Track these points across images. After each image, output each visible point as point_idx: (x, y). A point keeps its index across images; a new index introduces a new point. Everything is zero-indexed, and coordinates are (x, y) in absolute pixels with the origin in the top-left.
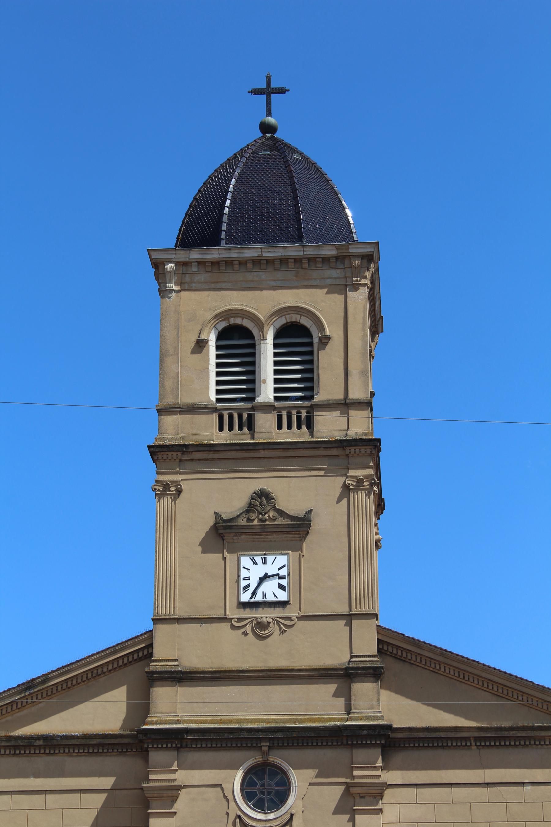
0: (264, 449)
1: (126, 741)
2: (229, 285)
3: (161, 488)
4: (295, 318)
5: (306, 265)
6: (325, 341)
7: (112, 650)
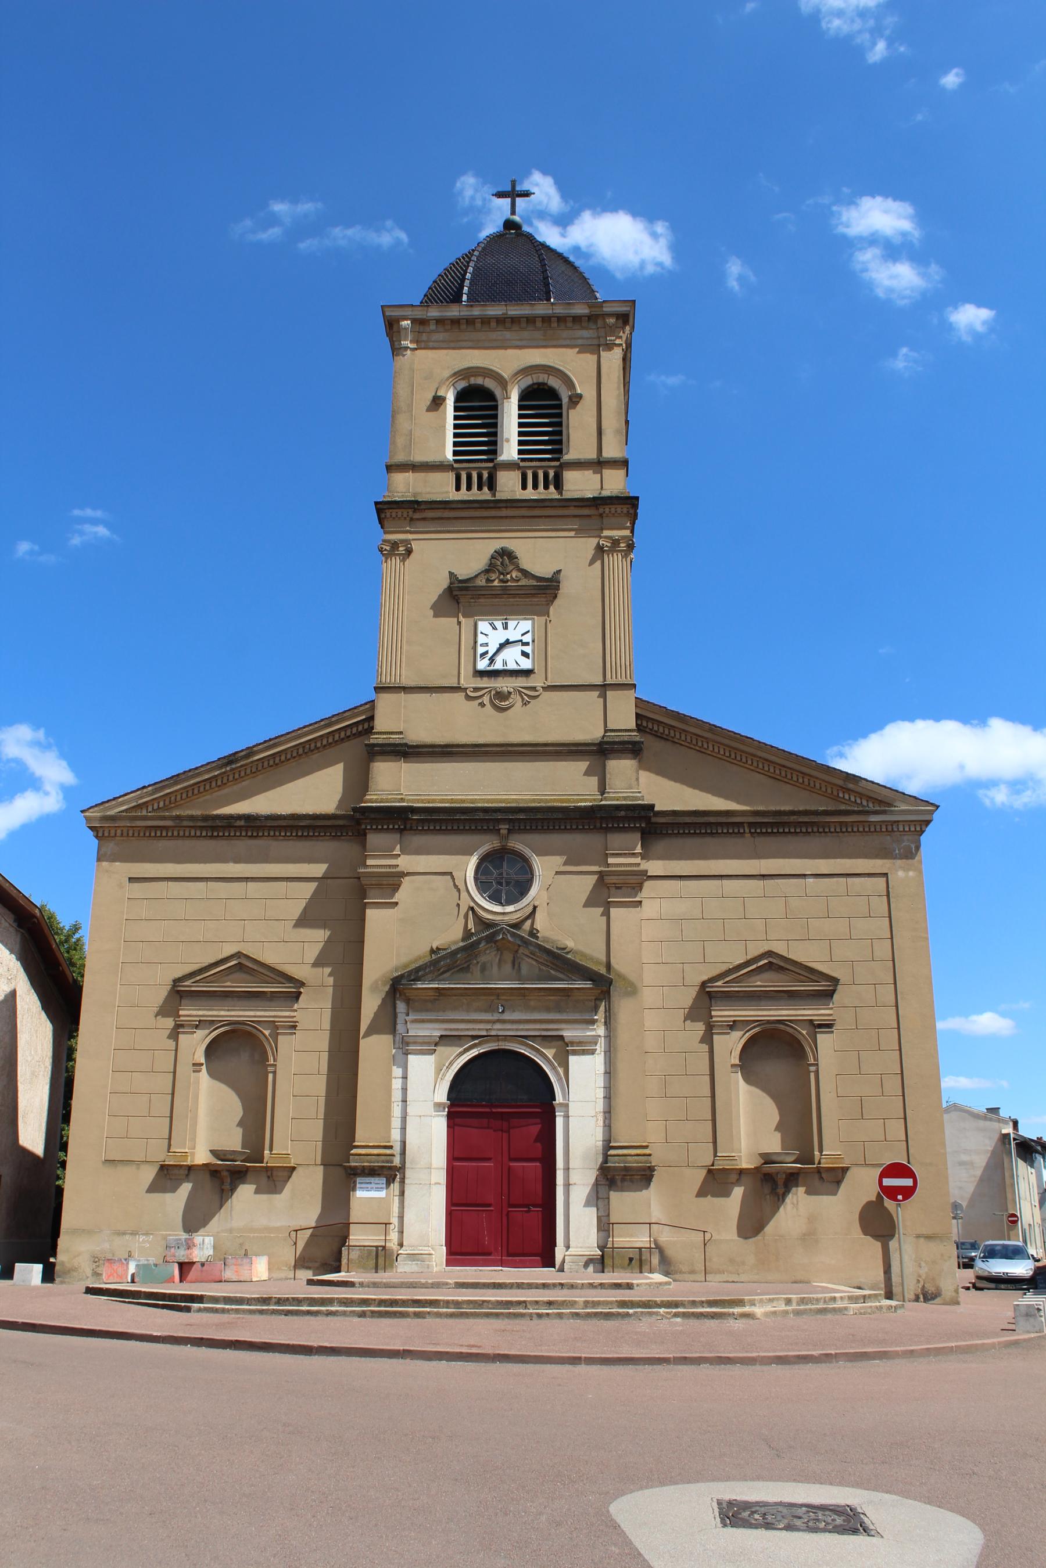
0: (506, 507)
1: (341, 822)
2: (470, 344)
3: (388, 548)
4: (542, 378)
5: (554, 325)
6: (576, 399)
7: (327, 722)
